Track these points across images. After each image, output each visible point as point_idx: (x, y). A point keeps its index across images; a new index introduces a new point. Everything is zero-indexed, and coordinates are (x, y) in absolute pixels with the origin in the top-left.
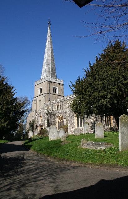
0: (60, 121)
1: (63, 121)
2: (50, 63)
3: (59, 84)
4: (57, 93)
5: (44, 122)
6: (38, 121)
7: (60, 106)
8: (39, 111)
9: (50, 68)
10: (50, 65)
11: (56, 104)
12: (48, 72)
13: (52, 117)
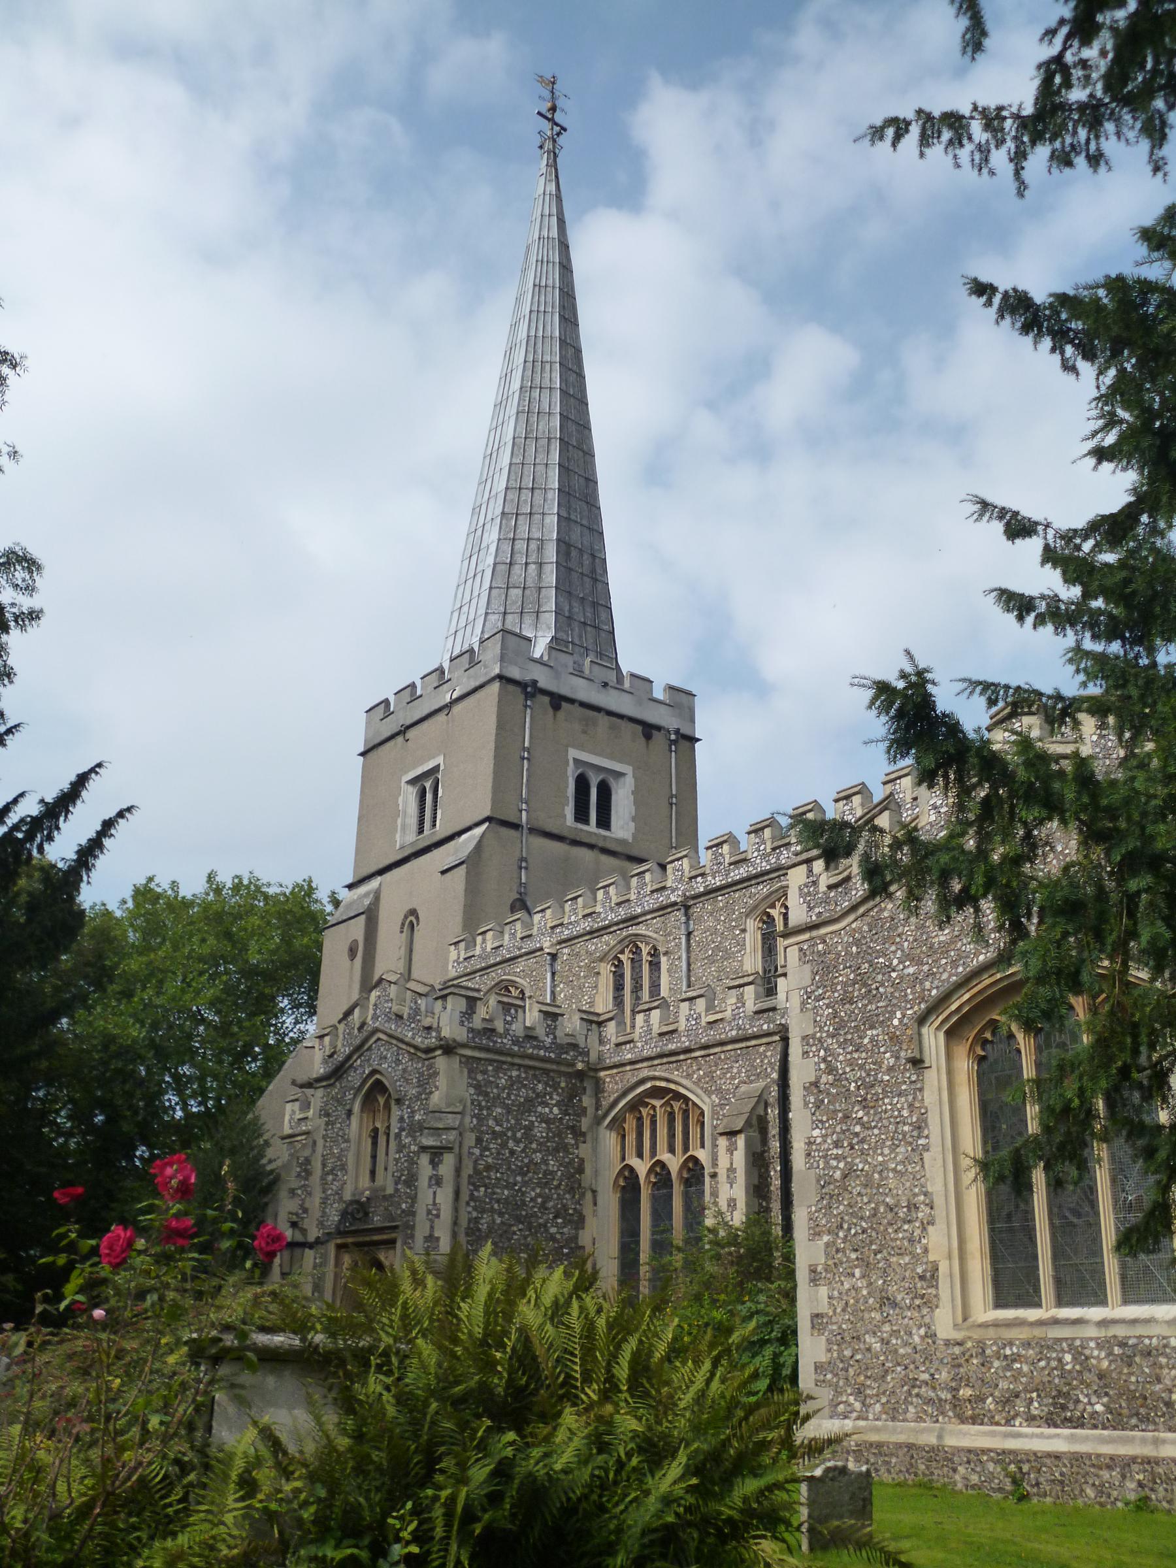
0: (642, 1167)
1: (694, 1172)
2: (554, 496)
3: (649, 730)
4: (622, 826)
5: (411, 1180)
7: (655, 966)
9: (551, 554)
10: (552, 521)
11: (608, 941)
12: (515, 593)
13: (528, 1106)
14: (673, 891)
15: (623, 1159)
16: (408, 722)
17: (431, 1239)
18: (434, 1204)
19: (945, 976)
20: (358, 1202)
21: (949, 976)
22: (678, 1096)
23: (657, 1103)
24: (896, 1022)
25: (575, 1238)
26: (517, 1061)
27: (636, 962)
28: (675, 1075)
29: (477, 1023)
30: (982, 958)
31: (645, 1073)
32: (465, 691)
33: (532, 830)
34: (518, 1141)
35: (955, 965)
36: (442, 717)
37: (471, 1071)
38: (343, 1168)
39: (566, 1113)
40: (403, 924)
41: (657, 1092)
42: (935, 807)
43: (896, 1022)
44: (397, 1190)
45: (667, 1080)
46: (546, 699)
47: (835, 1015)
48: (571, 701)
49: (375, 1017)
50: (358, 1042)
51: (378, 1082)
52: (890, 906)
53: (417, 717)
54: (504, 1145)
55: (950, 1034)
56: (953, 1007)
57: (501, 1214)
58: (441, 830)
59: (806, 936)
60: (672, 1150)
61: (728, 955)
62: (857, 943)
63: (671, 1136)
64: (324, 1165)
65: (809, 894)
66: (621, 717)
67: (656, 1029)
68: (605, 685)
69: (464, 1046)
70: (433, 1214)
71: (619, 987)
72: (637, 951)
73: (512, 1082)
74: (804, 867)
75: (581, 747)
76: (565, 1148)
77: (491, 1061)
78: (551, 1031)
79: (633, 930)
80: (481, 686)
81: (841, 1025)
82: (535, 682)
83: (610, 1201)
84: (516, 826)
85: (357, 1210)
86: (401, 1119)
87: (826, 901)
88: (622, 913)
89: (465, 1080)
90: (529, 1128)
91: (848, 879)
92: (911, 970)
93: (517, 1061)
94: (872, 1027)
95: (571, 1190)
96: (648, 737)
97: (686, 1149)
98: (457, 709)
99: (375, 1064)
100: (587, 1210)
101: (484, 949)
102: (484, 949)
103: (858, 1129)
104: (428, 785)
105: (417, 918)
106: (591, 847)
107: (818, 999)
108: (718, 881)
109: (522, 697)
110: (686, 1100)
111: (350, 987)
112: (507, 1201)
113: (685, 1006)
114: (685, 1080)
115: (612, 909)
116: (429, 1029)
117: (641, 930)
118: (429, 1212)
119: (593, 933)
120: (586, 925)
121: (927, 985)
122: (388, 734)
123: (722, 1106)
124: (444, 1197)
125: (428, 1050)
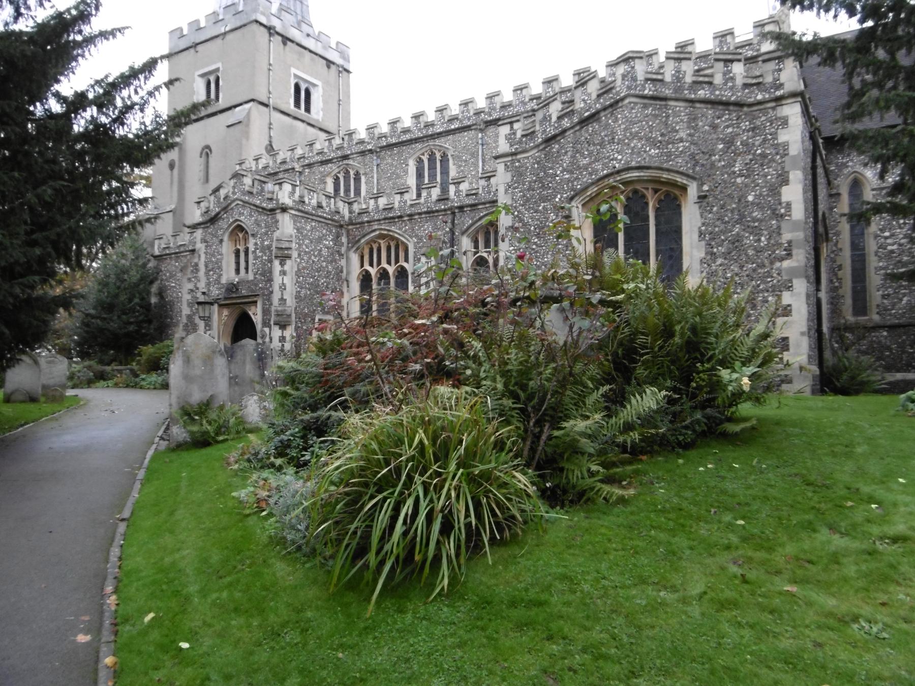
0: (373, 271)
3: (329, 63)
4: (318, 112)
6: (214, 267)
7: (357, 179)
8: (222, 193)
11: (333, 168)
13: (320, 240)
14: (369, 143)
15: (362, 266)
16: (198, 41)
17: (282, 300)
18: (283, 284)
19: (585, 180)
20: (232, 284)
21: (587, 179)
22: (393, 238)
23: (382, 242)
24: (557, 200)
25: (340, 302)
26: (314, 218)
28: (393, 228)
30: (605, 172)
31: (376, 227)
32: (234, 27)
33: (274, 109)
34: (316, 257)
35: (591, 174)
36: (219, 41)
37: (295, 221)
38: (220, 268)
39: (335, 244)
40: (201, 154)
42: (583, 100)
43: (557, 200)
44: (255, 278)
45: (389, 231)
46: (280, 38)
47: (524, 196)
48: (292, 41)
49: (234, 193)
50: (224, 205)
51: (239, 226)
52: (557, 146)
53: (203, 39)
54: (310, 258)
55: (583, 205)
56: (589, 193)
57: (309, 290)
58: (222, 103)
59: (510, 158)
60: (371, 265)
61: (398, 177)
62: (538, 163)
63: (389, 257)
64: (206, 266)
65: (511, 138)
66: (316, 54)
67: (381, 207)
68: (308, 35)
69: (292, 208)
70: (283, 287)
72: (347, 173)
73: (313, 228)
74: (508, 126)
75: (298, 69)
76: (335, 261)
77: (303, 217)
78: (329, 205)
79: (346, 162)
80: (245, 25)
81: (528, 200)
82: (274, 28)
83: (355, 286)
84: (266, 105)
85: (232, 288)
86: (256, 244)
87: (520, 142)
88: (339, 153)
89: (292, 226)
90: (320, 250)
91: (533, 132)
92: (567, 176)
93: (314, 218)
94: (544, 202)
95: (338, 280)
96: (329, 67)
97: (397, 261)
98: (229, 37)
99: (237, 217)
100: (345, 289)
101: (257, 168)
102: (257, 168)
103: (534, 247)
104: (212, 79)
105: (211, 150)
106: (303, 121)
107: (514, 188)
108: (394, 141)
109: (267, 35)
110: (397, 239)
111: (172, 183)
112: (312, 284)
113: (399, 196)
114: (396, 230)
115: (333, 151)
116: (271, 199)
117: (351, 162)
118: (280, 287)
119: (323, 163)
120: (318, 158)
121: (575, 183)
122: (184, 47)
123: (418, 243)
124: (287, 280)
125: (272, 210)
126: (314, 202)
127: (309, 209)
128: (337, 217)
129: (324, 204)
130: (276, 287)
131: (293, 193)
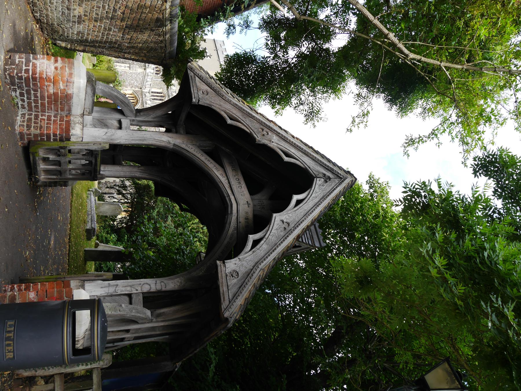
22: (137, 104)
27: (161, 96)
28: (140, 104)
29: (149, 74)
31: (140, 99)
36: (217, 59)
41: (137, 101)
67: (147, 101)
70: (121, 66)
71: (158, 93)
78: (148, 85)
124: (123, 68)
126: (148, 80)
127: (146, 77)
128: (144, 87)
129: (148, 83)
130: (120, 64)
131: (151, 73)
